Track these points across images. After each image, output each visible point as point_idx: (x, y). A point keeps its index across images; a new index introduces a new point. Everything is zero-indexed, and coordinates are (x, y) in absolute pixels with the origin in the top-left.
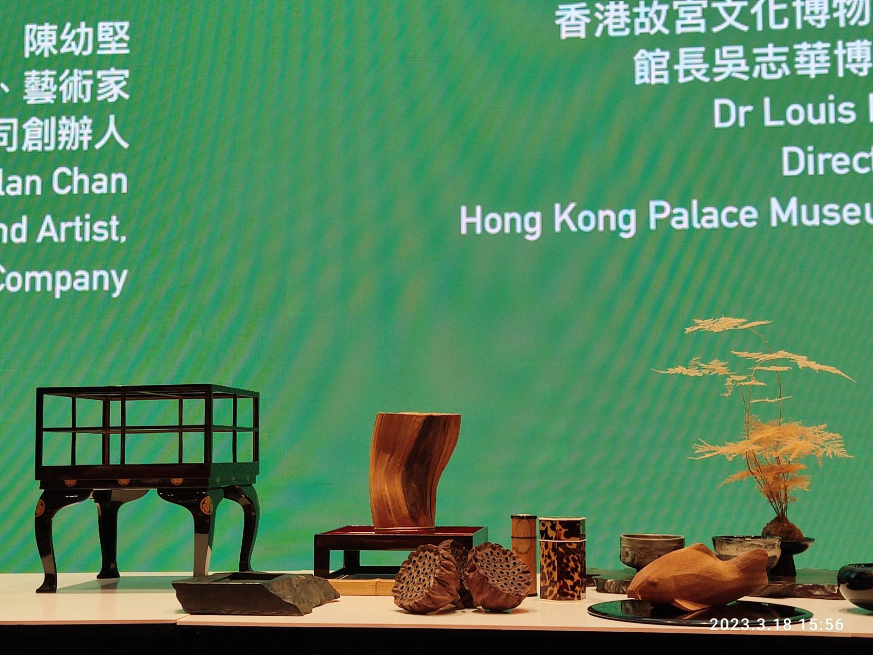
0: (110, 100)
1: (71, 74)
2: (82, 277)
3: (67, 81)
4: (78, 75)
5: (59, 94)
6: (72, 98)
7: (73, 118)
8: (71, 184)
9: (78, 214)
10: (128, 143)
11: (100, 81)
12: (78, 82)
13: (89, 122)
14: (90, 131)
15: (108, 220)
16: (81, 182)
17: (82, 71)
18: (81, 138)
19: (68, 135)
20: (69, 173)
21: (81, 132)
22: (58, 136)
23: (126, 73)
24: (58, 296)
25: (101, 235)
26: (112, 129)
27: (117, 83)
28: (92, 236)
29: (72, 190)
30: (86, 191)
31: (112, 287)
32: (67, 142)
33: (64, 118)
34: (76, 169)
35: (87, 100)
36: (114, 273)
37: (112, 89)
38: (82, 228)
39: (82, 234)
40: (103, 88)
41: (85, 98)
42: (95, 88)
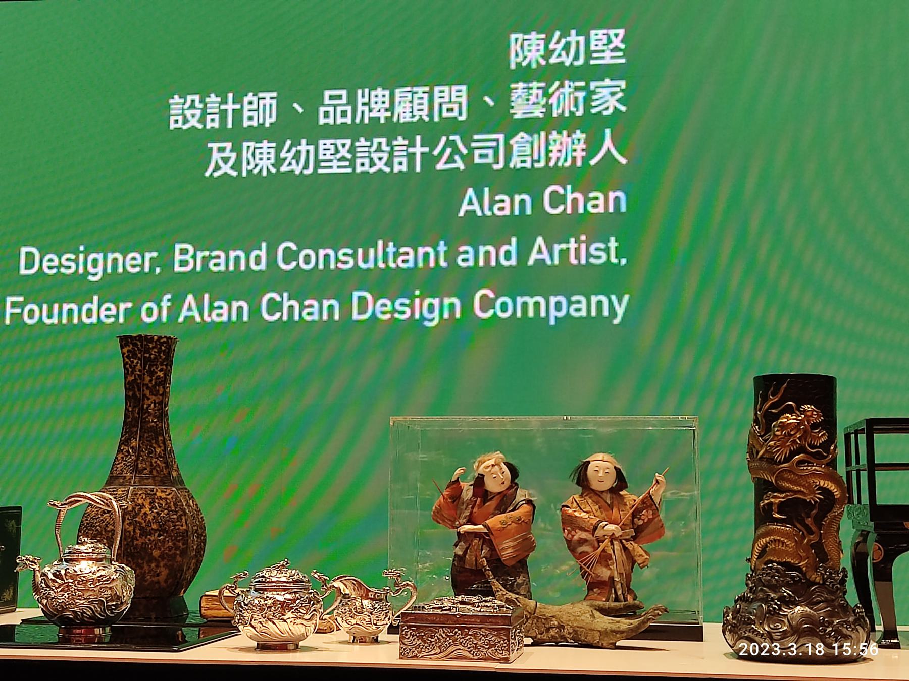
0: (605, 113)
1: (562, 86)
2: (579, 302)
3: (557, 94)
4: (570, 87)
5: (549, 107)
6: (563, 112)
7: (565, 133)
8: (564, 203)
9: (572, 236)
10: (627, 159)
11: (594, 93)
12: (570, 94)
13: (583, 136)
14: (584, 147)
15: (607, 241)
16: (575, 201)
17: (573, 82)
18: (574, 154)
19: (560, 151)
20: (561, 191)
21: (574, 147)
22: (548, 152)
23: (623, 84)
24: (552, 322)
25: (599, 257)
26: (608, 143)
27: (613, 94)
29: (565, 210)
30: (581, 211)
32: (558, 159)
33: (554, 132)
34: (569, 187)
35: (580, 113)
36: (613, 297)
37: (607, 101)
38: (577, 250)
39: (578, 257)
40: (597, 100)
41: (577, 111)
42: (588, 101)
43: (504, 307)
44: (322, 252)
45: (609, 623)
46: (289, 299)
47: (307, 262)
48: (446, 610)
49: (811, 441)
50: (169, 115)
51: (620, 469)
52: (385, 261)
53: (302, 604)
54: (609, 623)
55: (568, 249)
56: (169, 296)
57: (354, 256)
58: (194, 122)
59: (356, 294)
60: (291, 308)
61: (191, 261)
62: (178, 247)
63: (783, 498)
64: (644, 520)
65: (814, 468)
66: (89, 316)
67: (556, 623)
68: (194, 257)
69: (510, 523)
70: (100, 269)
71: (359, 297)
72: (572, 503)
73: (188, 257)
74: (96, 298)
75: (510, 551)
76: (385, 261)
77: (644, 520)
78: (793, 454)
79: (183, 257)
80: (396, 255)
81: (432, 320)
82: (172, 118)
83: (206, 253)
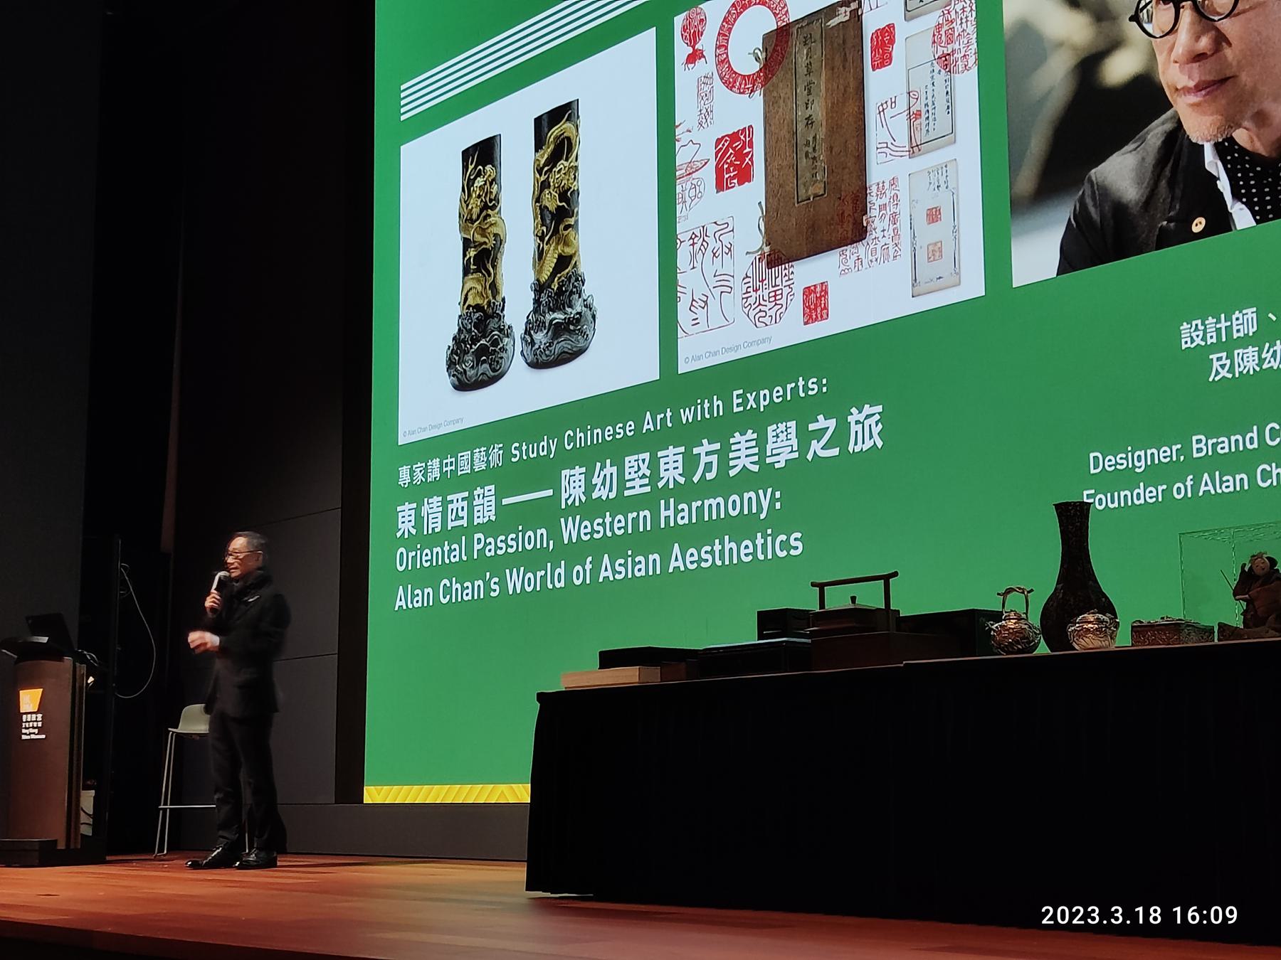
50: (1181, 338)
56: (1191, 477)
58: (1198, 341)
62: (1195, 438)
66: (1138, 499)
70: (1143, 462)
74: (1142, 484)
79: (1199, 446)
82: (1183, 341)
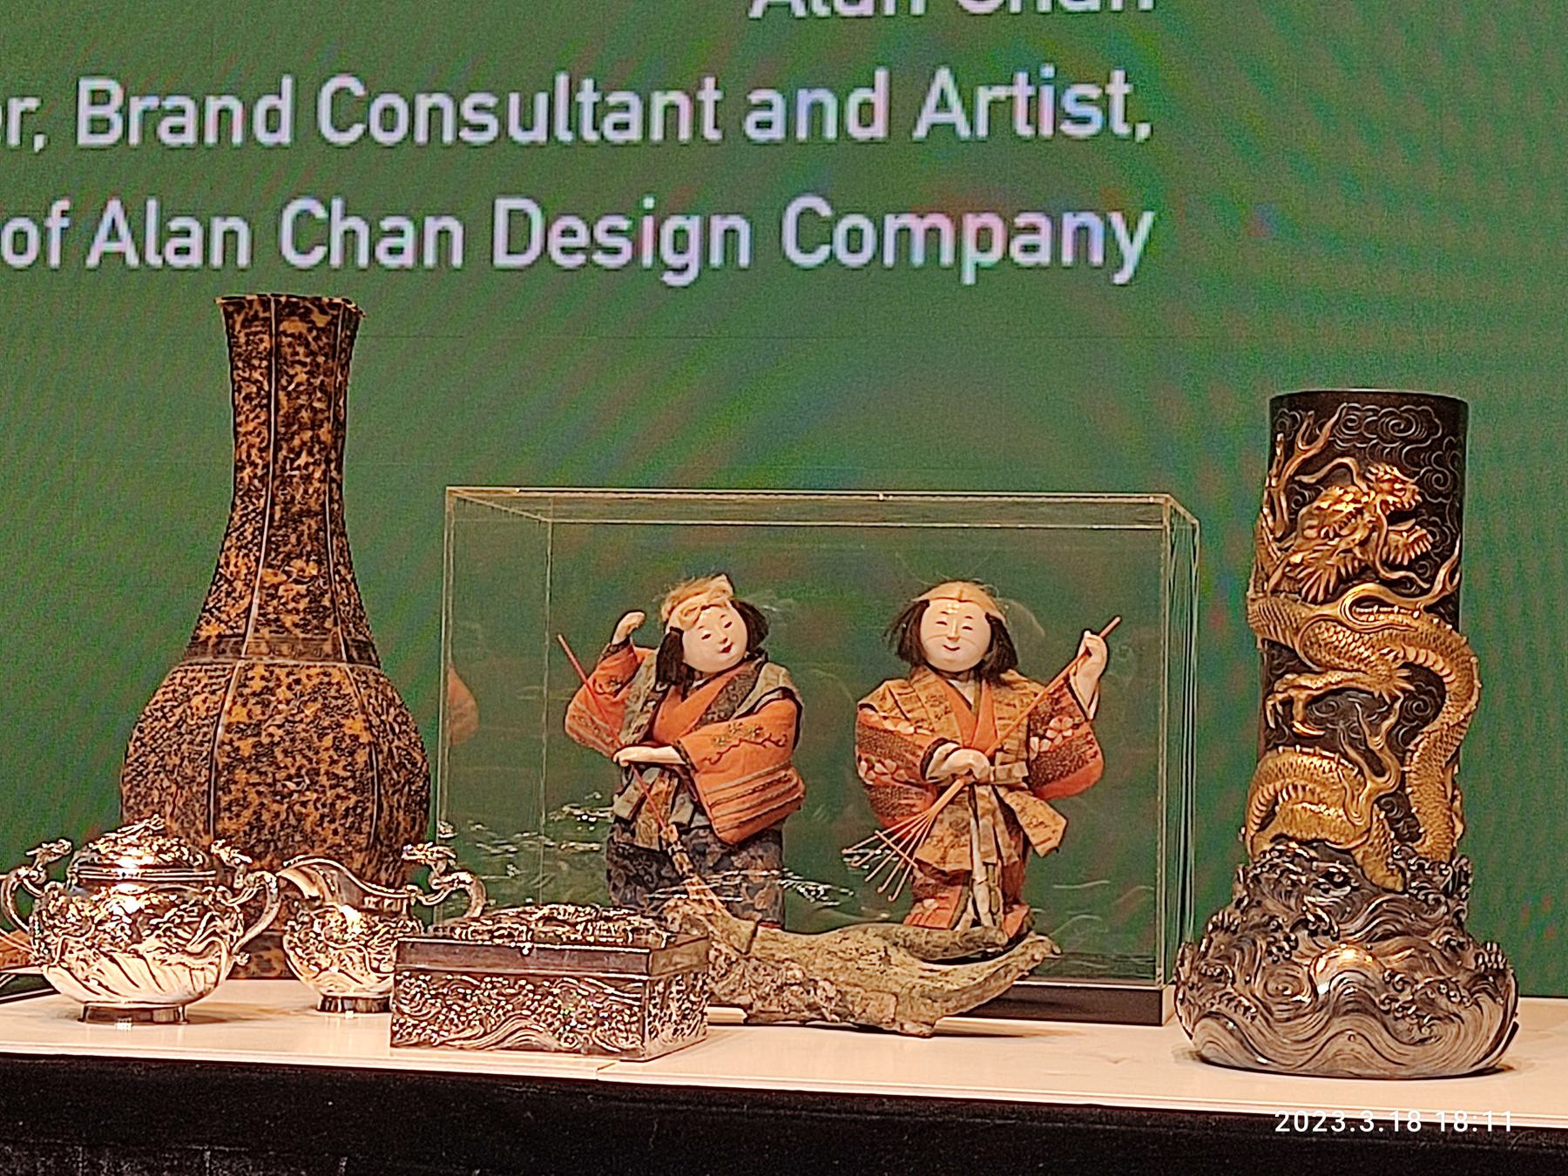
24: (969, 278)
28: (1060, 124)
31: (1114, 257)
36: (1116, 219)
38: (1033, 102)
39: (1033, 119)
43: (854, 240)
44: (424, 103)
45: (922, 977)
46: (346, 215)
47: (389, 125)
48: (501, 936)
49: (1389, 554)
51: (999, 621)
52: (574, 125)
53: (181, 917)
54: (922, 977)
55: (1011, 98)
57: (501, 113)
59: (503, 205)
60: (350, 234)
61: (117, 122)
63: (1317, 689)
64: (1052, 740)
65: (1392, 617)
67: (799, 975)
68: (124, 112)
69: (737, 742)
71: (511, 212)
72: (884, 698)
73: (110, 111)
75: (734, 806)
76: (574, 125)
77: (1052, 740)
78: (1345, 583)
79: (99, 111)
80: (600, 110)
81: (683, 269)
83: (152, 102)
